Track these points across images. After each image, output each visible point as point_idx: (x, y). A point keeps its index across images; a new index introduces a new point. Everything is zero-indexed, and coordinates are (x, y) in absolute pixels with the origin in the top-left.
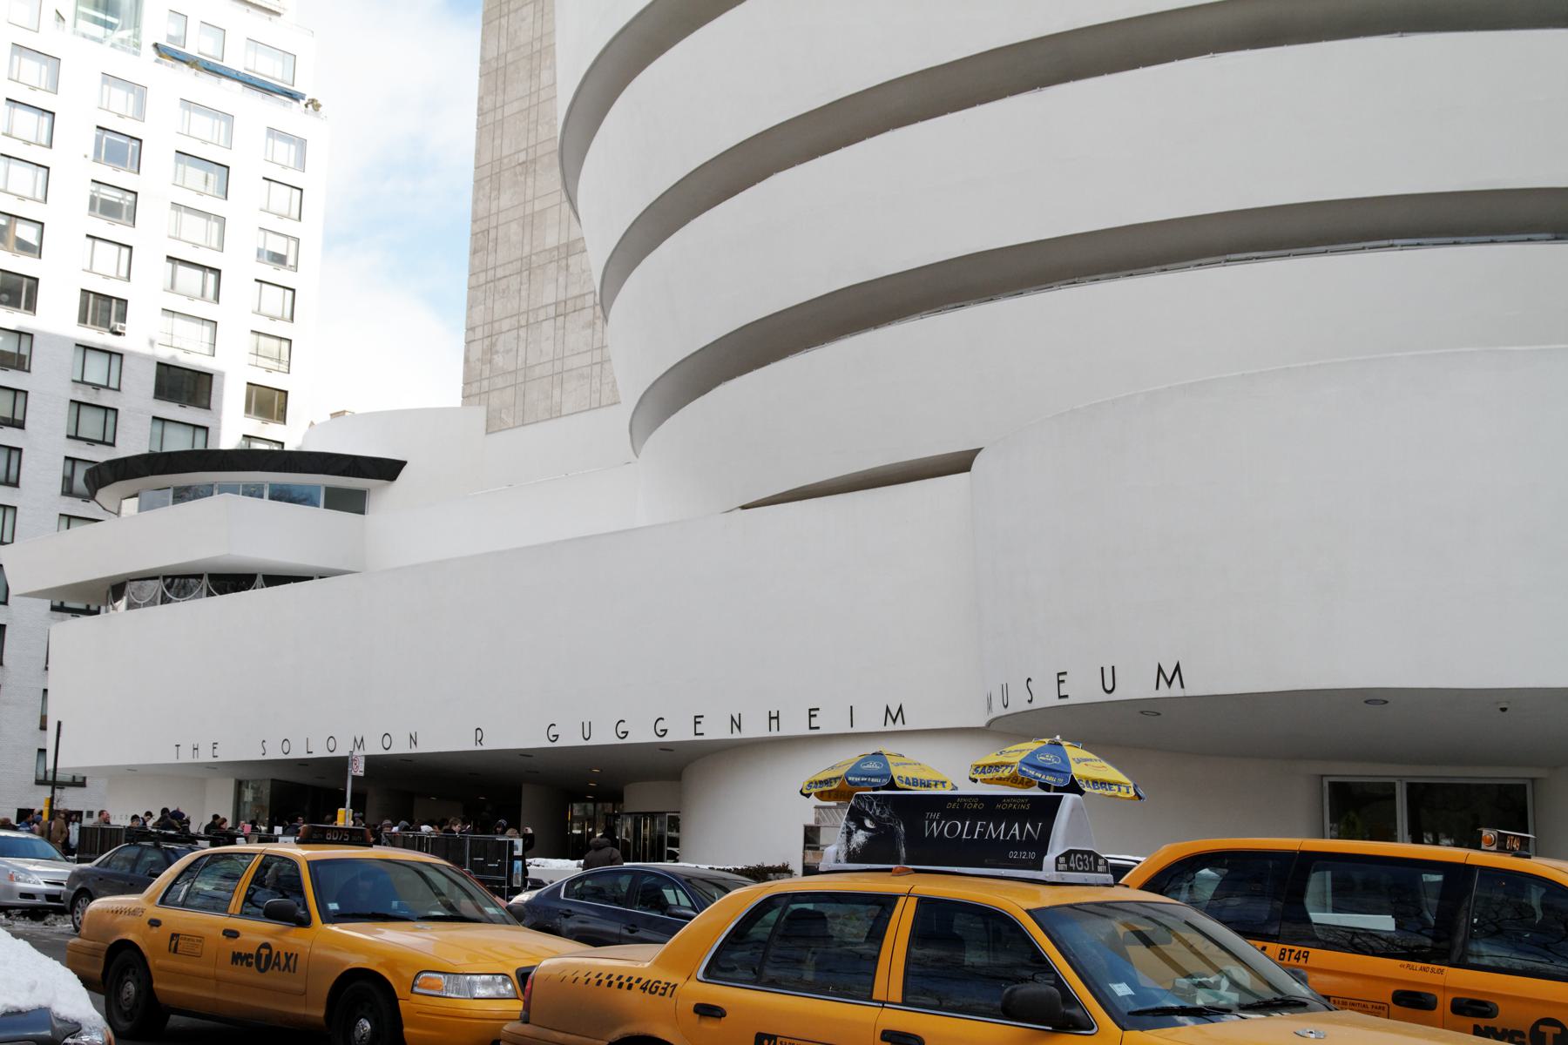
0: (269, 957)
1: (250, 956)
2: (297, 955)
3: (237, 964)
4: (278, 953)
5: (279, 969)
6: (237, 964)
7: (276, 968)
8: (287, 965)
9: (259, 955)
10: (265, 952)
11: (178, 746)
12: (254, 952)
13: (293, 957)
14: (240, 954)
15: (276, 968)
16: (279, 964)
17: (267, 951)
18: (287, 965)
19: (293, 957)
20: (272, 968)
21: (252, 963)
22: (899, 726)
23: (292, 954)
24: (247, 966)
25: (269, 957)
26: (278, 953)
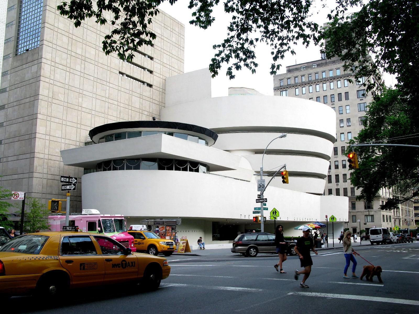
0: (126, 264)
1: (119, 264)
2: (135, 262)
3: (114, 267)
4: (129, 262)
5: (130, 267)
6: (114, 267)
7: (129, 266)
8: (132, 265)
9: (122, 264)
10: (124, 262)
11: (241, 215)
12: (120, 263)
13: (134, 263)
14: (115, 264)
15: (129, 266)
16: (129, 265)
17: (125, 262)
18: (132, 265)
19: (134, 263)
20: (128, 267)
21: (120, 266)
22: (316, 221)
23: (133, 262)
24: (118, 267)
25: (126, 264)
26: (129, 262)
